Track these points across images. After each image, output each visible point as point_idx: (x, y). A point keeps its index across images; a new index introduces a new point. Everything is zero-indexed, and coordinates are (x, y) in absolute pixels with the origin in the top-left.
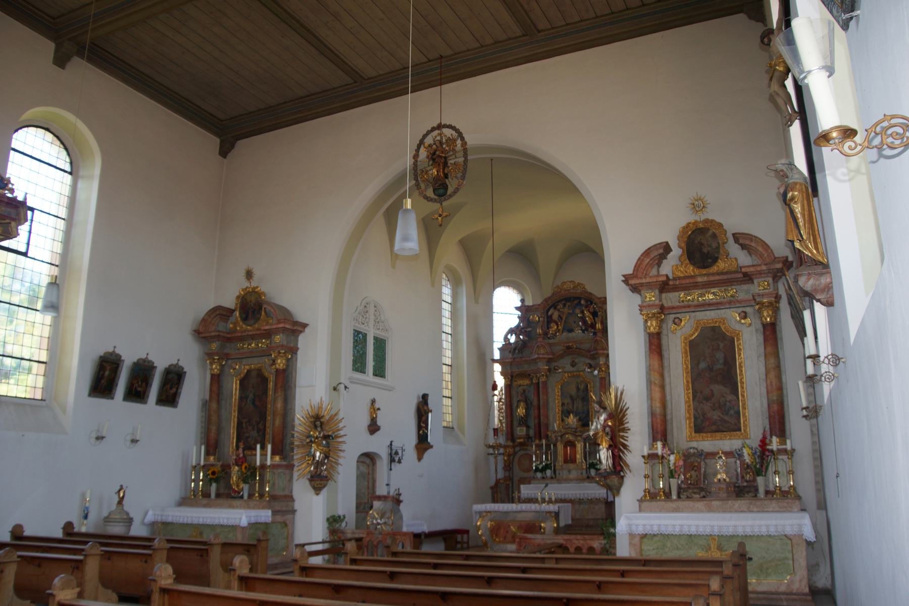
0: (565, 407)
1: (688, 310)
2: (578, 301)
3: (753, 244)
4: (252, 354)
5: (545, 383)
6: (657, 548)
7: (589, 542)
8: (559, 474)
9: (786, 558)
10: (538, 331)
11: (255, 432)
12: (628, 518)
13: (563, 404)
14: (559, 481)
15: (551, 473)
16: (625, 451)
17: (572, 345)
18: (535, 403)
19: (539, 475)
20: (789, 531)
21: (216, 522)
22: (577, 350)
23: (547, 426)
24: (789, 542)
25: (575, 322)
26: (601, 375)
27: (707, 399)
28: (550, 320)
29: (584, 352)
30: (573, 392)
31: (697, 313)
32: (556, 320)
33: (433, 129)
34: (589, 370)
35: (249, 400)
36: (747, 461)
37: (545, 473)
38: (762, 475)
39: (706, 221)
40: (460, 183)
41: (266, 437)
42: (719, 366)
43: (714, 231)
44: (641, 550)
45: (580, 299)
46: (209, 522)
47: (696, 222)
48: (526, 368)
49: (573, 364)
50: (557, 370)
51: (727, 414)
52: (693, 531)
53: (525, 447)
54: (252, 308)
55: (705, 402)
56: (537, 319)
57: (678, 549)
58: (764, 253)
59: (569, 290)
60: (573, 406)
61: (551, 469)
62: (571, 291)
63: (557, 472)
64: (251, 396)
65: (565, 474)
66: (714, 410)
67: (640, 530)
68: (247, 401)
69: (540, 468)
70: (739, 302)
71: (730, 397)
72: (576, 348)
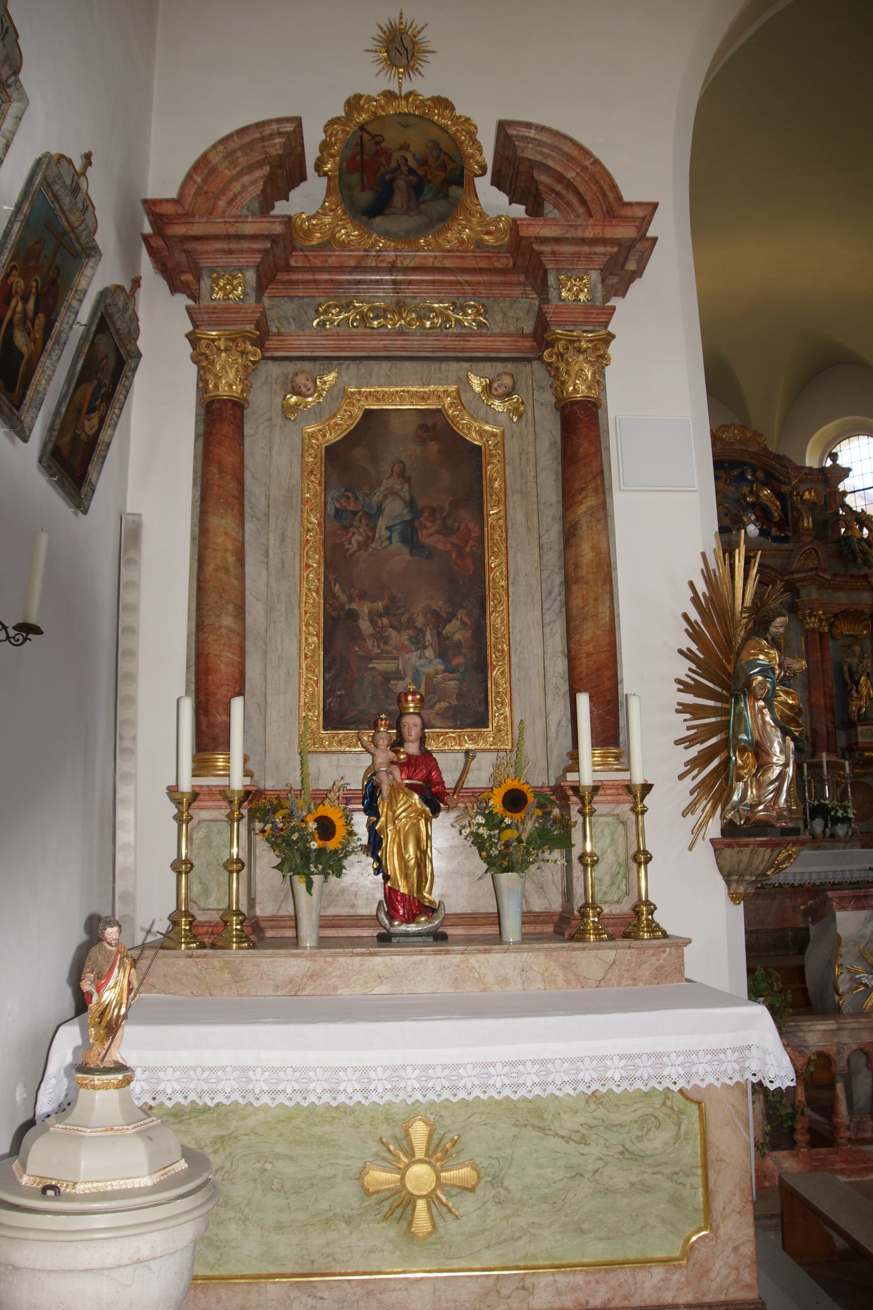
2: (740, 470)
11: (429, 653)
25: (726, 515)
35: (382, 523)
54: (411, 171)
59: (732, 443)
62: (736, 447)
64: (395, 509)
68: (374, 530)
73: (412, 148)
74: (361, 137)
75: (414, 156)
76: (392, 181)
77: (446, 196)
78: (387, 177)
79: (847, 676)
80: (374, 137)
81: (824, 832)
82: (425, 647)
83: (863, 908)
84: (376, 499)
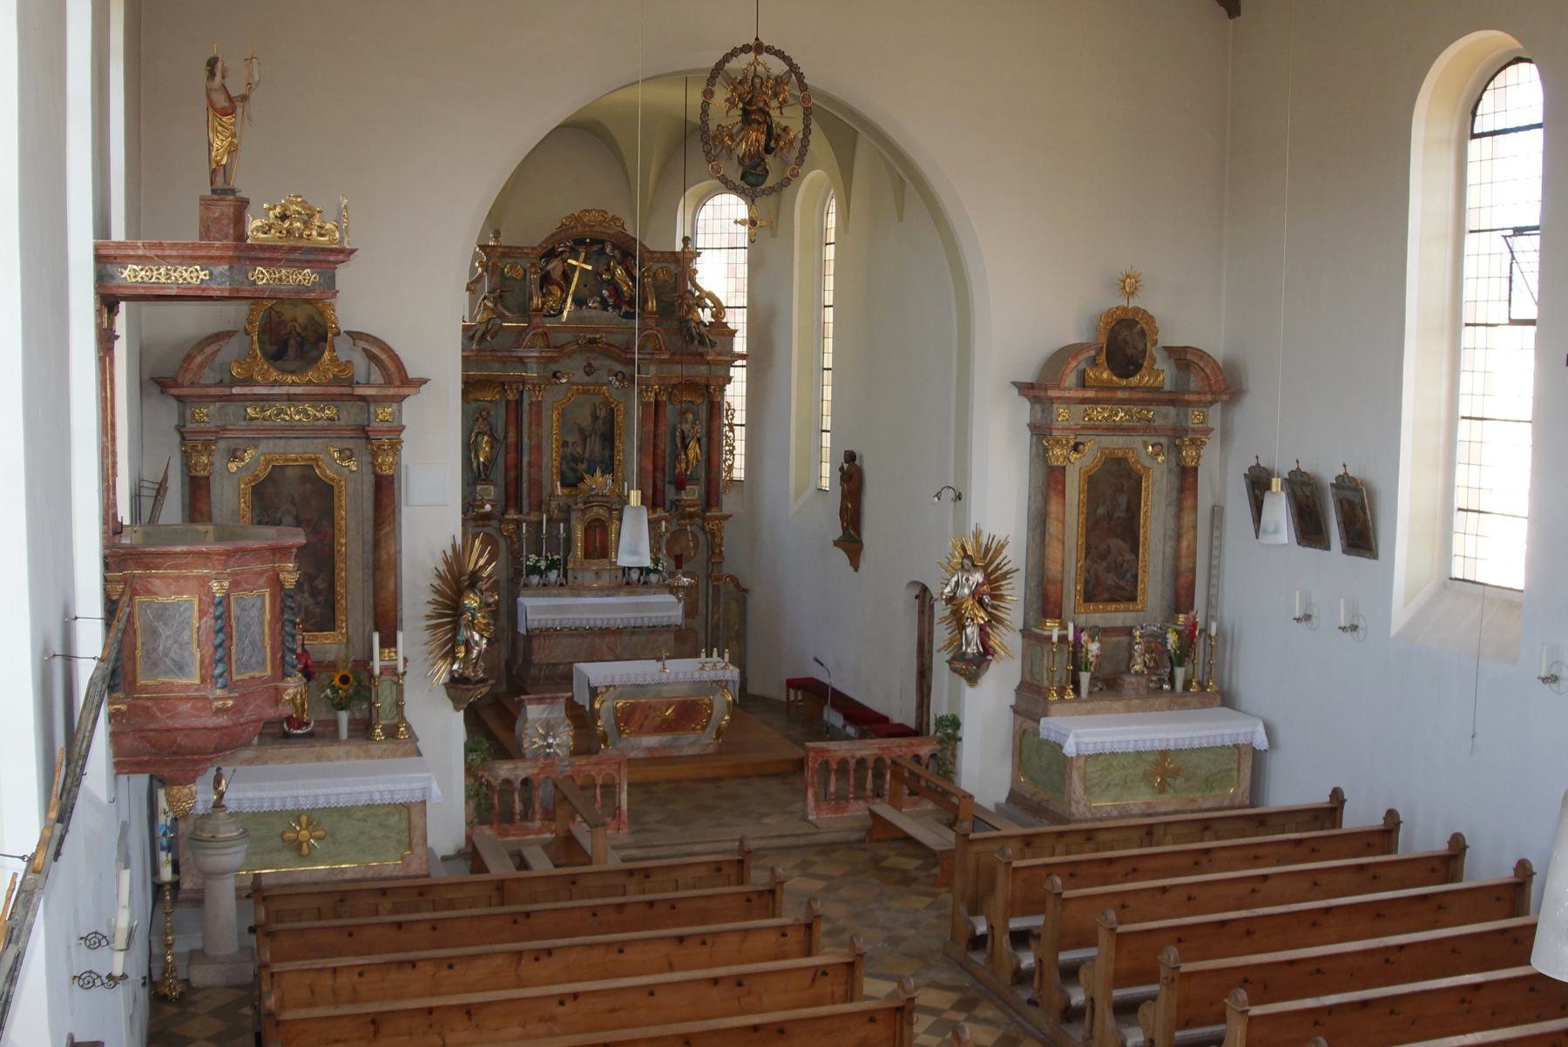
0: (569, 450)
1: (1090, 432)
2: (601, 246)
3: (1201, 364)
4: (290, 431)
5: (537, 406)
6: (1101, 770)
7: (914, 749)
8: (576, 578)
9: (1231, 770)
10: (535, 301)
11: (306, 595)
12: (1077, 735)
13: (565, 444)
14: (578, 591)
15: (559, 576)
16: (1000, 627)
17: (600, 338)
18: (512, 438)
19: (535, 579)
20: (1241, 740)
21: (364, 800)
22: (605, 346)
23: (537, 485)
24: (1236, 751)
25: (585, 285)
26: (649, 397)
27: (1103, 557)
28: (546, 279)
29: (617, 351)
30: (586, 422)
31: (1103, 438)
32: (559, 279)
33: (746, 49)
34: (617, 383)
36: (1169, 648)
37: (546, 576)
38: (1184, 666)
39: (1136, 310)
40: (796, 171)
41: (337, 606)
42: (1120, 513)
43: (1144, 326)
44: (1085, 773)
45: (602, 242)
46: (343, 802)
47: (1125, 310)
48: (495, 371)
49: (589, 370)
50: (559, 379)
51: (1123, 578)
52: (1148, 746)
53: (486, 522)
54: (298, 334)
55: (1099, 561)
56: (521, 271)
57: (1124, 768)
58: (1212, 378)
59: (593, 226)
60: (584, 452)
61: (559, 570)
62: (595, 229)
63: (570, 573)
65: (587, 578)
66: (1109, 572)
67: (1090, 750)
69: (543, 568)
70: (1155, 429)
71: (1129, 556)
72: (607, 344)
73: (300, 321)
74: (270, 313)
75: (300, 325)
76: (288, 339)
77: (318, 348)
78: (285, 337)
79: (678, 440)
80: (277, 312)
81: (639, 580)
82: (303, 592)
83: (542, 704)
84: (278, 515)
